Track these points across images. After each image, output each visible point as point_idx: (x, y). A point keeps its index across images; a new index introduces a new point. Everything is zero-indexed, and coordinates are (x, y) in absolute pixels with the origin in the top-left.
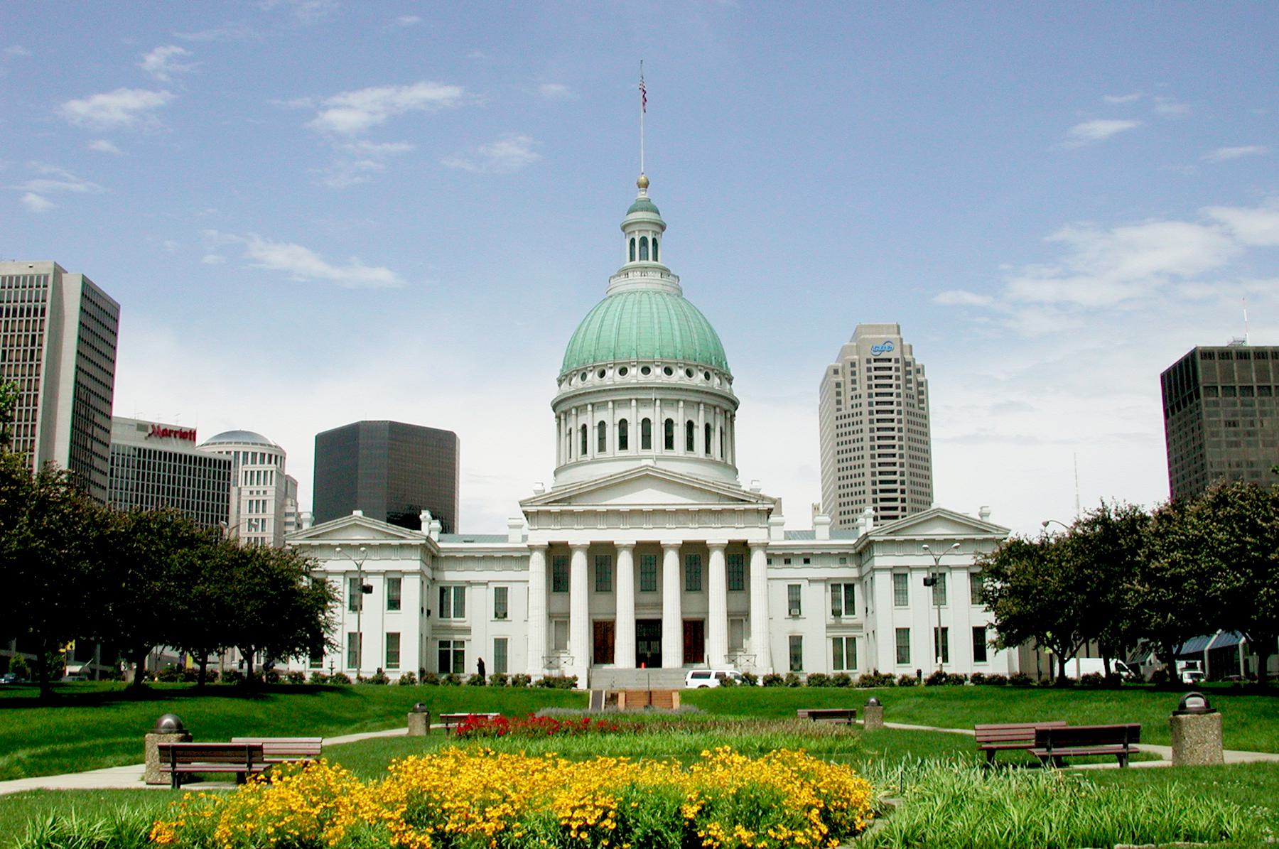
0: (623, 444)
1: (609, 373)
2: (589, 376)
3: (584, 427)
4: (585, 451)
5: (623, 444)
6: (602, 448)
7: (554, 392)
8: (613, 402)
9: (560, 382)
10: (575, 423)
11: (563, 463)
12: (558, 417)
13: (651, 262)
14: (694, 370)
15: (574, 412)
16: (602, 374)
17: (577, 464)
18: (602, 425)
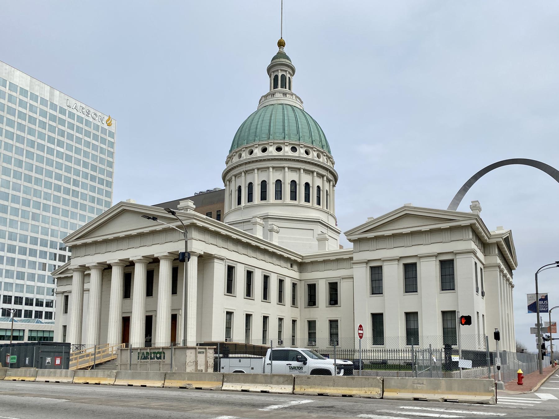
0: (279, 195)
5: (279, 195)
6: (264, 197)
9: (230, 158)
10: (243, 182)
11: (233, 208)
15: (243, 174)
18: (264, 184)
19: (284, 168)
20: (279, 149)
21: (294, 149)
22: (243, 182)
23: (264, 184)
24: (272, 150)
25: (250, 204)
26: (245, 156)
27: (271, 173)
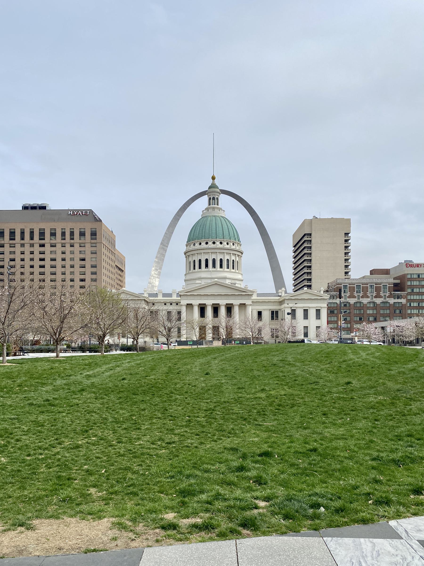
0: (207, 266)
1: (202, 244)
2: (196, 245)
3: (194, 261)
4: (194, 269)
5: (207, 266)
6: (200, 268)
7: (184, 249)
8: (204, 253)
9: (187, 246)
12: (186, 257)
13: (216, 206)
14: (229, 242)
16: (200, 244)
17: (192, 273)
18: (200, 261)
19: (209, 253)
20: (207, 243)
21: (214, 243)
22: (191, 260)
23: (200, 261)
24: (203, 244)
25: (194, 271)
26: (192, 247)
27: (203, 256)
